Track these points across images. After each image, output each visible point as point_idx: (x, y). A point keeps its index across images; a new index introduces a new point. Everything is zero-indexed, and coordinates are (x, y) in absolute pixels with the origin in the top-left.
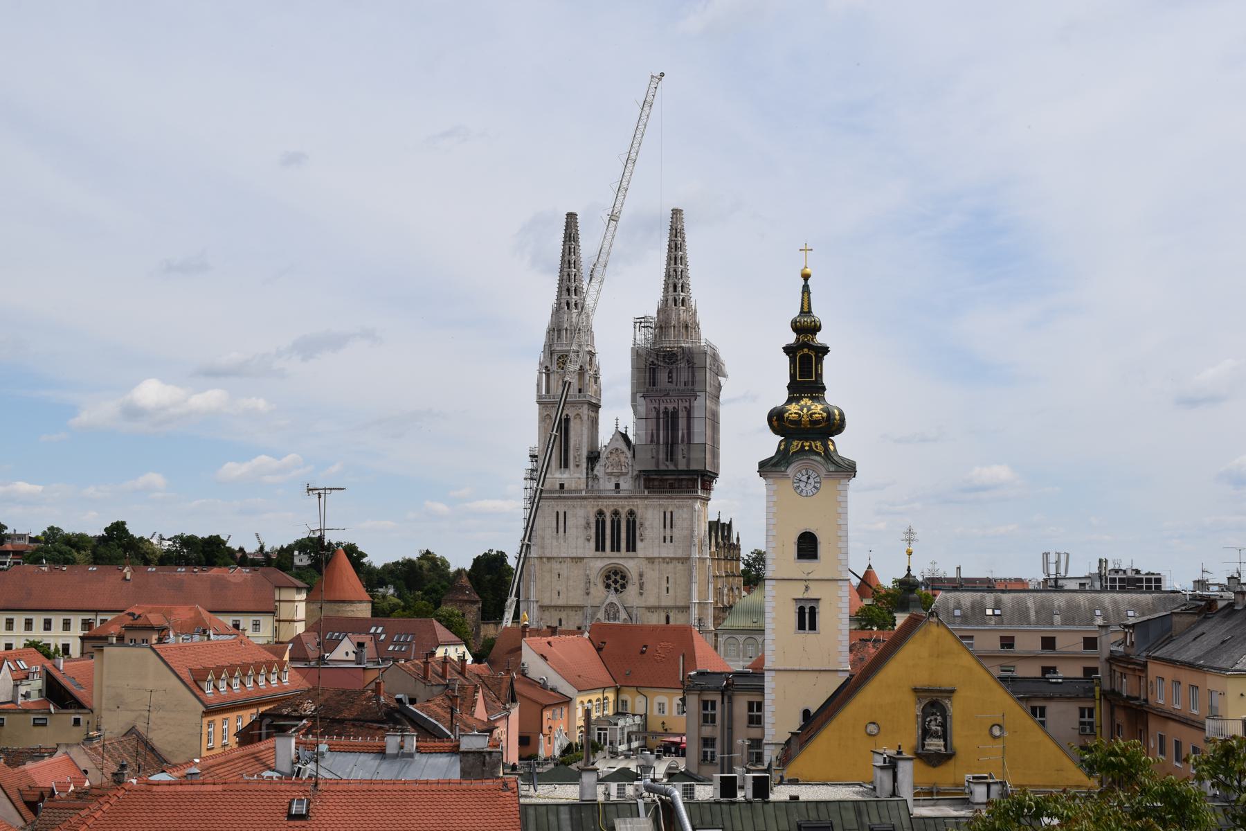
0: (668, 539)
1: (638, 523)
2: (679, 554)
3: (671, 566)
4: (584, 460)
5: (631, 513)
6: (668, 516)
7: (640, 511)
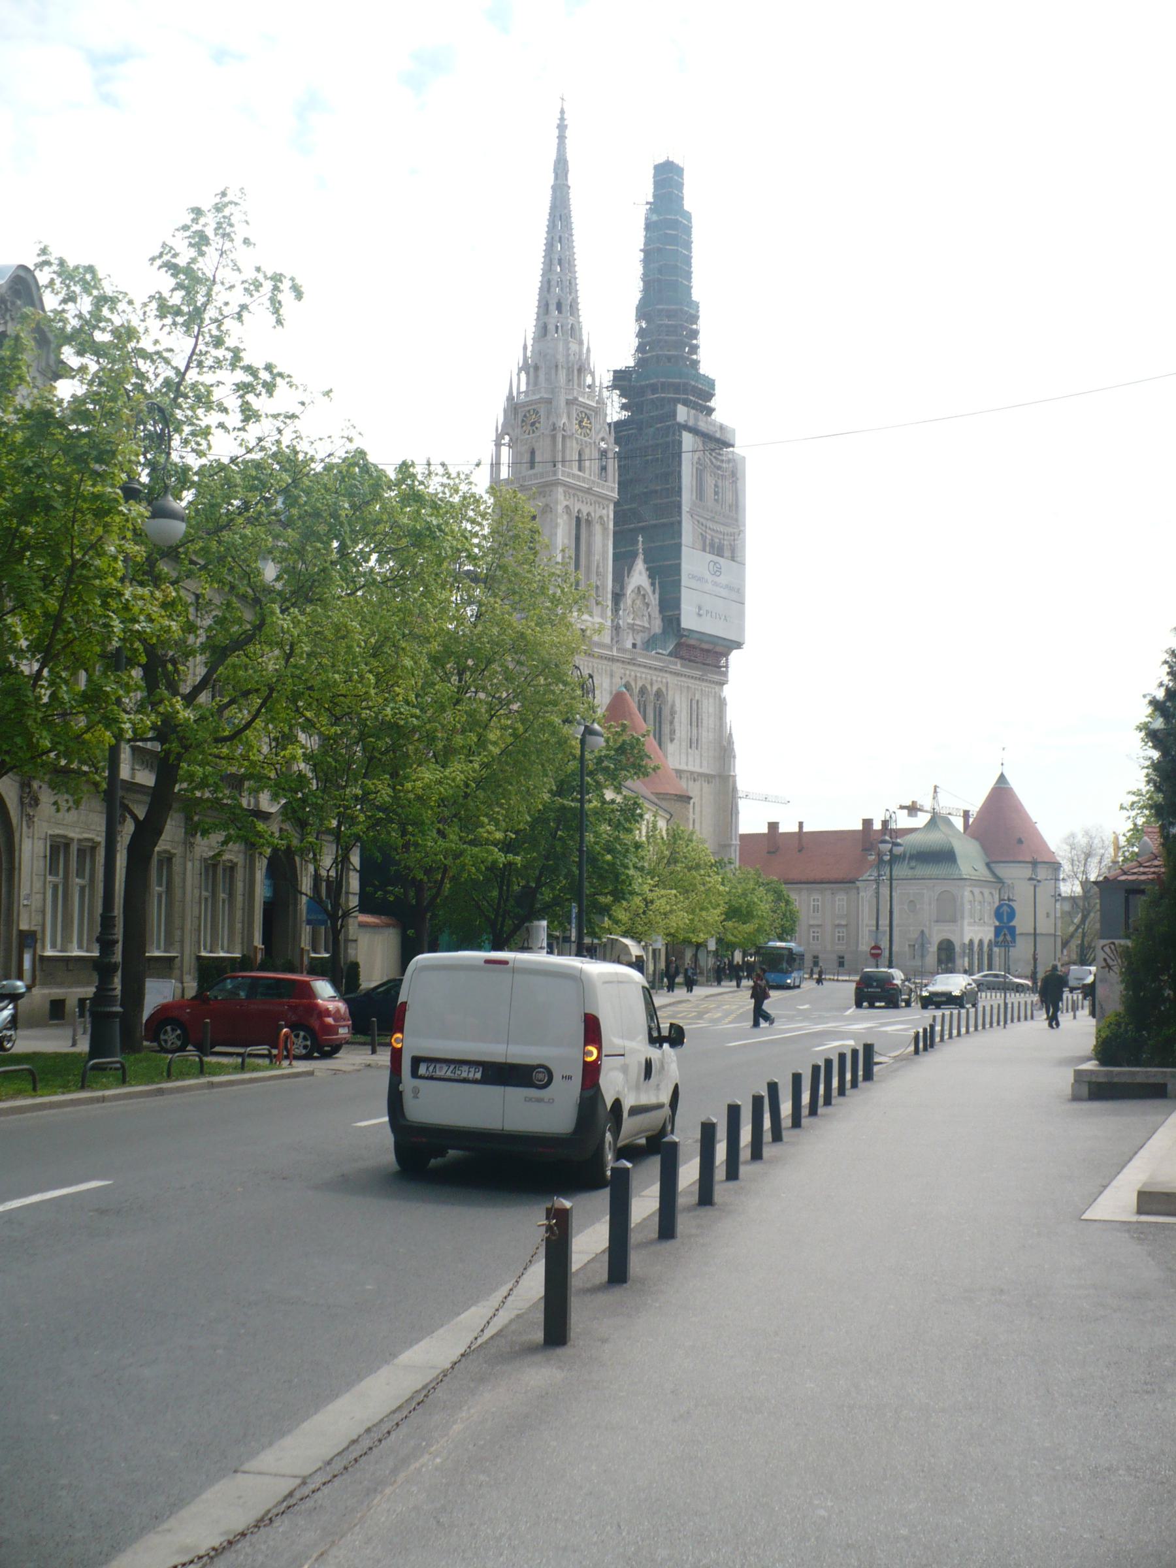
0: (694, 745)
1: (666, 712)
2: (705, 770)
3: (698, 783)
4: (610, 596)
5: (659, 694)
6: (695, 706)
7: (670, 693)
